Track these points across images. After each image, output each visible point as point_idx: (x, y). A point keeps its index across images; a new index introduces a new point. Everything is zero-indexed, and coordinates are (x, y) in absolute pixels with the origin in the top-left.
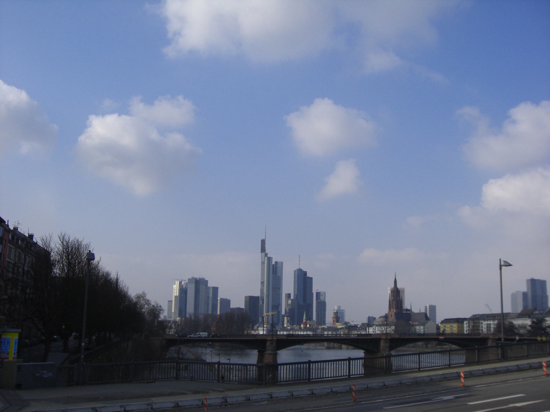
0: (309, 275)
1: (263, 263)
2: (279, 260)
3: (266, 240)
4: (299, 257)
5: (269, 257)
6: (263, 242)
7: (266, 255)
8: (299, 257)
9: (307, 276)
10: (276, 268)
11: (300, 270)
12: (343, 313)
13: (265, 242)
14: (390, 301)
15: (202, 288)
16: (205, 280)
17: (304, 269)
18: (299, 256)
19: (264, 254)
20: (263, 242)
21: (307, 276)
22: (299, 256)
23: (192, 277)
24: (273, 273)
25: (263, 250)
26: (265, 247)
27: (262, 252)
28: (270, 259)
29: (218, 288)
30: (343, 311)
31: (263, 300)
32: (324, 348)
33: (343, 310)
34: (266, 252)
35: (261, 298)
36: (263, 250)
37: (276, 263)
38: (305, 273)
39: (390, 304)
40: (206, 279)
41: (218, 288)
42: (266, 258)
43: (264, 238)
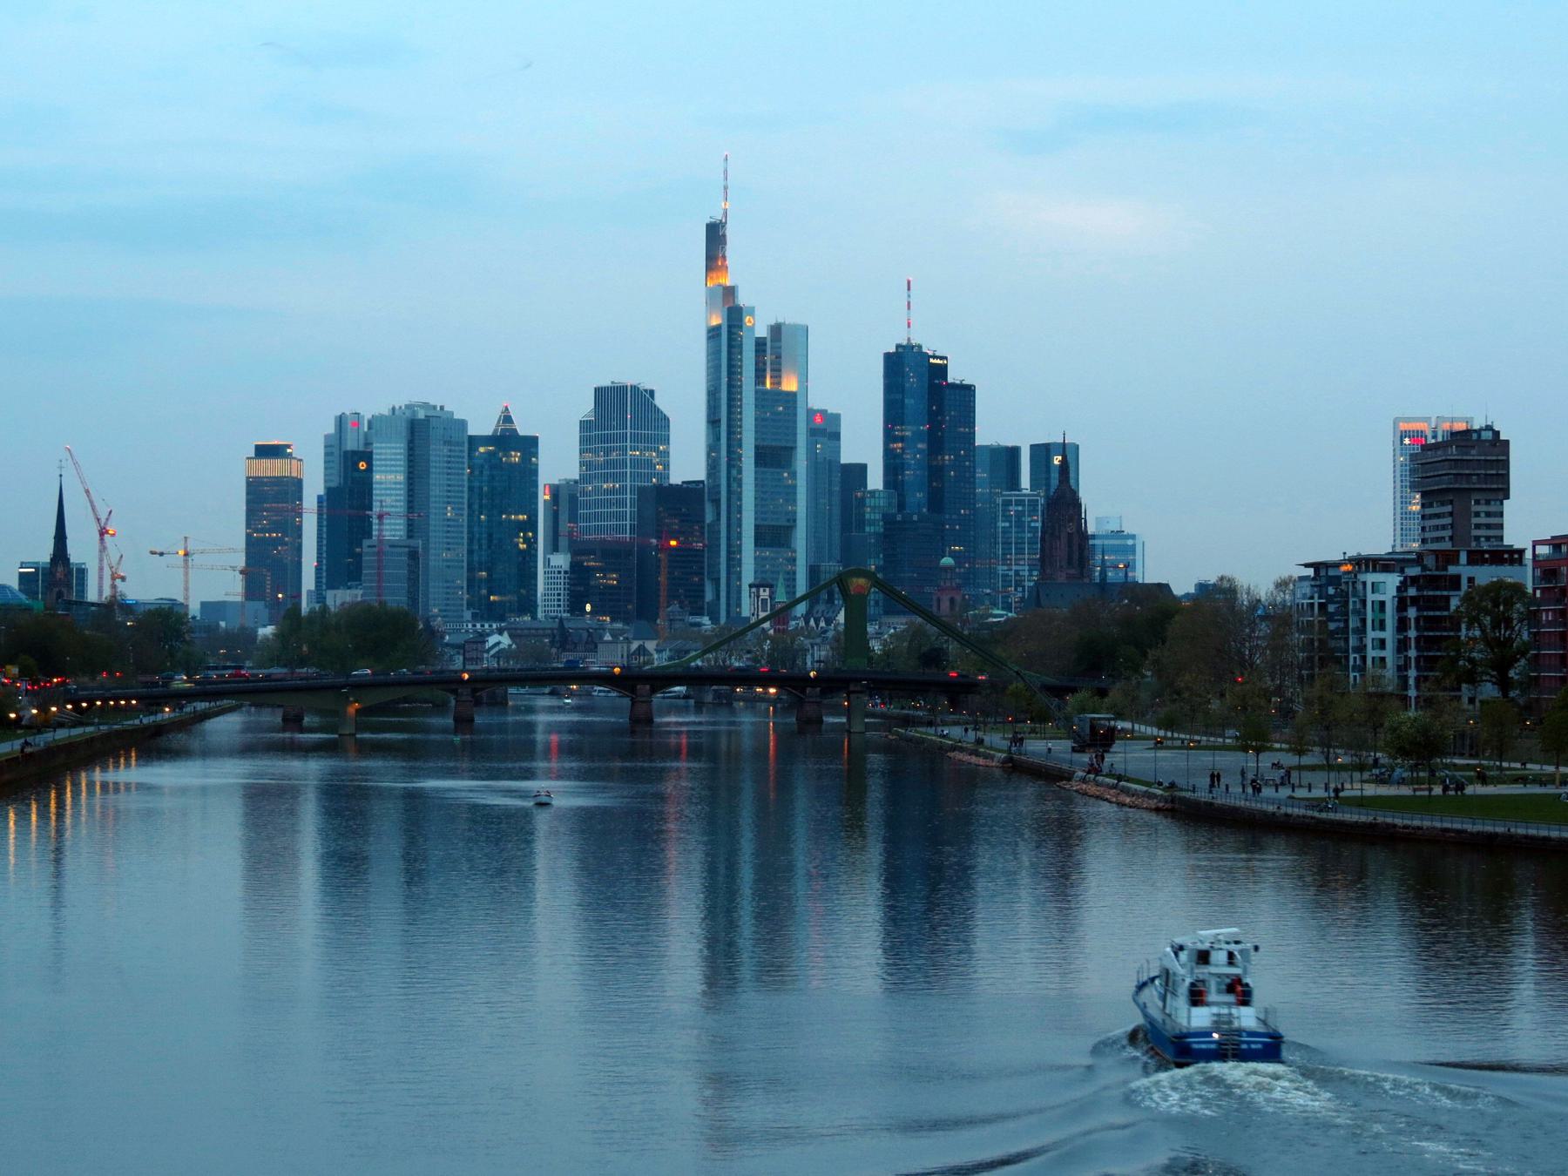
1: (713, 333)
2: (788, 317)
3: (728, 226)
9: (950, 380)
15: (437, 454)
17: (931, 343)
18: (909, 282)
21: (950, 380)
22: (909, 282)
23: (394, 409)
28: (735, 315)
30: (1130, 542)
31: (717, 502)
33: (1133, 537)
37: (776, 330)
40: (455, 417)
43: (719, 217)
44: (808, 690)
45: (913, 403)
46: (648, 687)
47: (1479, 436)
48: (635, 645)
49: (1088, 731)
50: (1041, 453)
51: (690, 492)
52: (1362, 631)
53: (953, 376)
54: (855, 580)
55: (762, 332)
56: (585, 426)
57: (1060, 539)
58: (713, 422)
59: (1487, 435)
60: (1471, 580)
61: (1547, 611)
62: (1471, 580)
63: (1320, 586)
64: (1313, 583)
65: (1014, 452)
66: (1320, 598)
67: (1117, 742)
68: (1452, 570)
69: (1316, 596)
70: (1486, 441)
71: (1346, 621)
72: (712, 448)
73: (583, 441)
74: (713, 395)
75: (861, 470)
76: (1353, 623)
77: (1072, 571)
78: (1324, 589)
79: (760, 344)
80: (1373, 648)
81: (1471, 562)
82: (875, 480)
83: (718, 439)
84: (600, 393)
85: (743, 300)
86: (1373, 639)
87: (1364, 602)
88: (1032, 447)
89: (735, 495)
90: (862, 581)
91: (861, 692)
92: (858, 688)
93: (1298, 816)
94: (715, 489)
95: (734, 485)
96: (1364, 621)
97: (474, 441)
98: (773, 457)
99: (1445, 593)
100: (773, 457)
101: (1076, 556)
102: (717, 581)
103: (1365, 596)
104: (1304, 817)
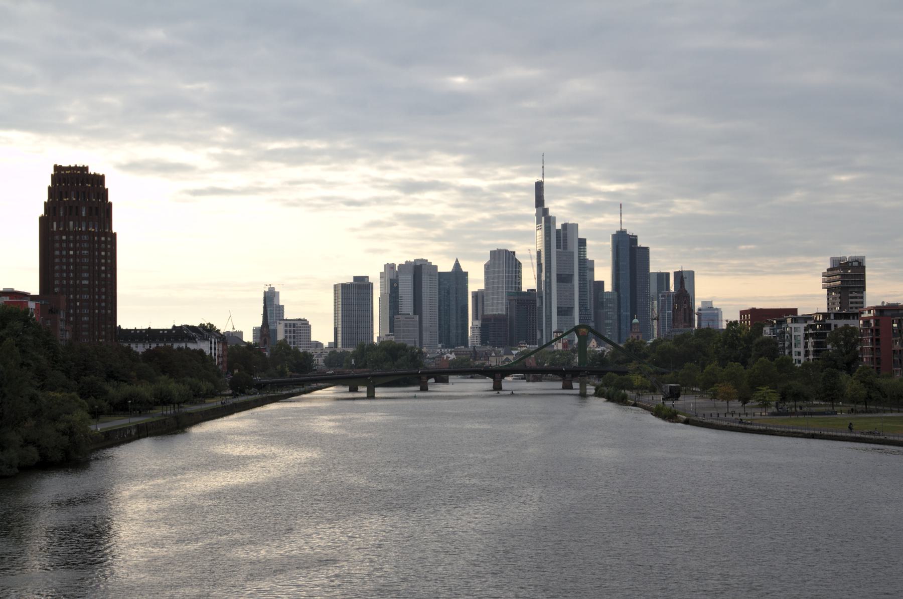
0: (641, 243)
4: (621, 208)
5: (550, 217)
7: (546, 211)
8: (621, 208)
10: (565, 236)
12: (717, 315)
13: (543, 187)
15: (425, 279)
16: (431, 265)
17: (630, 232)
18: (621, 205)
19: (541, 209)
21: (639, 246)
22: (621, 205)
24: (558, 247)
25: (540, 202)
26: (543, 196)
27: (537, 207)
30: (716, 312)
32: (525, 381)
33: (717, 309)
34: (545, 207)
35: (538, 295)
36: (540, 202)
37: (565, 226)
38: (633, 239)
40: (433, 264)
42: (543, 218)
43: (540, 179)
44: (566, 375)
46: (500, 375)
47: (852, 264)
48: (505, 357)
49: (669, 391)
52: (790, 346)
54: (581, 329)
55: (558, 226)
57: (680, 310)
59: (855, 264)
60: (836, 326)
61: (866, 338)
62: (836, 326)
63: (773, 329)
64: (771, 328)
65: (668, 275)
66: (773, 334)
67: (681, 396)
68: (827, 322)
69: (772, 333)
70: (855, 266)
71: (784, 344)
72: (539, 277)
75: (601, 283)
76: (787, 344)
77: (686, 324)
78: (775, 331)
79: (558, 231)
80: (795, 355)
81: (835, 318)
82: (608, 288)
83: (542, 271)
85: (551, 212)
86: (795, 352)
87: (791, 336)
88: (675, 273)
89: (549, 294)
90: (584, 330)
91: (585, 376)
92: (583, 375)
93: (735, 427)
95: (548, 291)
96: (791, 343)
97: (440, 273)
99: (824, 331)
100: (564, 279)
101: (687, 318)
102: (542, 331)
103: (791, 333)
104: (738, 427)
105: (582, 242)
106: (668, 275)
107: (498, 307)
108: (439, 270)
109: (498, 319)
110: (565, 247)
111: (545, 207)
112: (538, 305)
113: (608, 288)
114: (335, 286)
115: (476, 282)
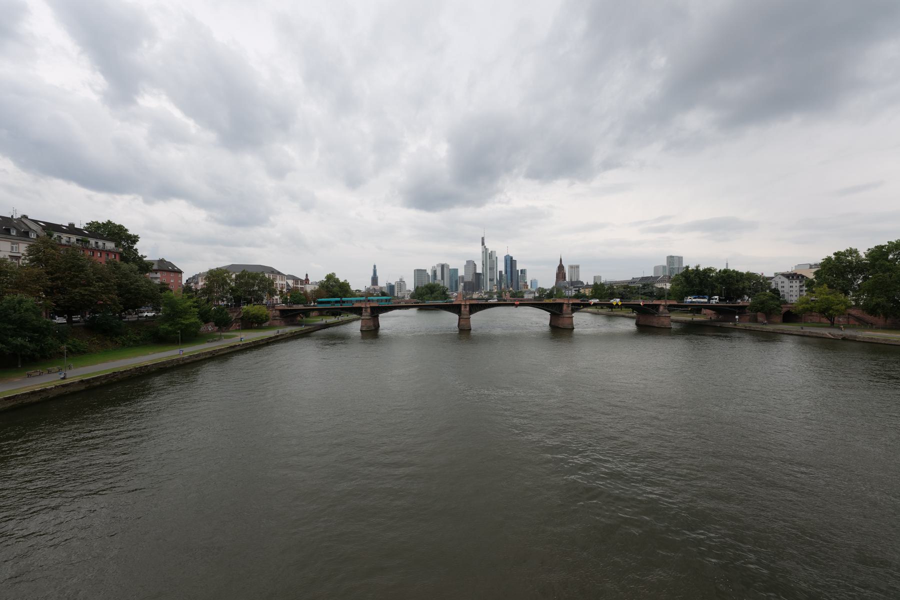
1: (483, 252)
2: (493, 250)
6: (483, 239)
7: (485, 247)
10: (492, 256)
11: (508, 255)
14: (557, 274)
15: (445, 269)
17: (511, 255)
20: (483, 239)
25: (483, 244)
28: (486, 249)
29: (457, 269)
36: (483, 244)
37: (491, 252)
38: (512, 258)
39: (557, 276)
41: (457, 269)
43: (483, 236)
45: (509, 262)
48: (480, 294)
50: (522, 271)
51: (479, 274)
53: (513, 259)
55: (490, 252)
56: (465, 266)
58: (483, 265)
65: (518, 270)
73: (465, 268)
74: (483, 262)
75: (501, 272)
82: (503, 273)
84: (467, 261)
85: (487, 247)
94: (483, 273)
98: (491, 269)
102: (484, 286)
105: (497, 258)
106: (518, 270)
107: (469, 279)
108: (450, 268)
109: (469, 282)
110: (492, 258)
111: (485, 245)
112: (482, 277)
113: (503, 273)
114: (415, 270)
115: (461, 273)
